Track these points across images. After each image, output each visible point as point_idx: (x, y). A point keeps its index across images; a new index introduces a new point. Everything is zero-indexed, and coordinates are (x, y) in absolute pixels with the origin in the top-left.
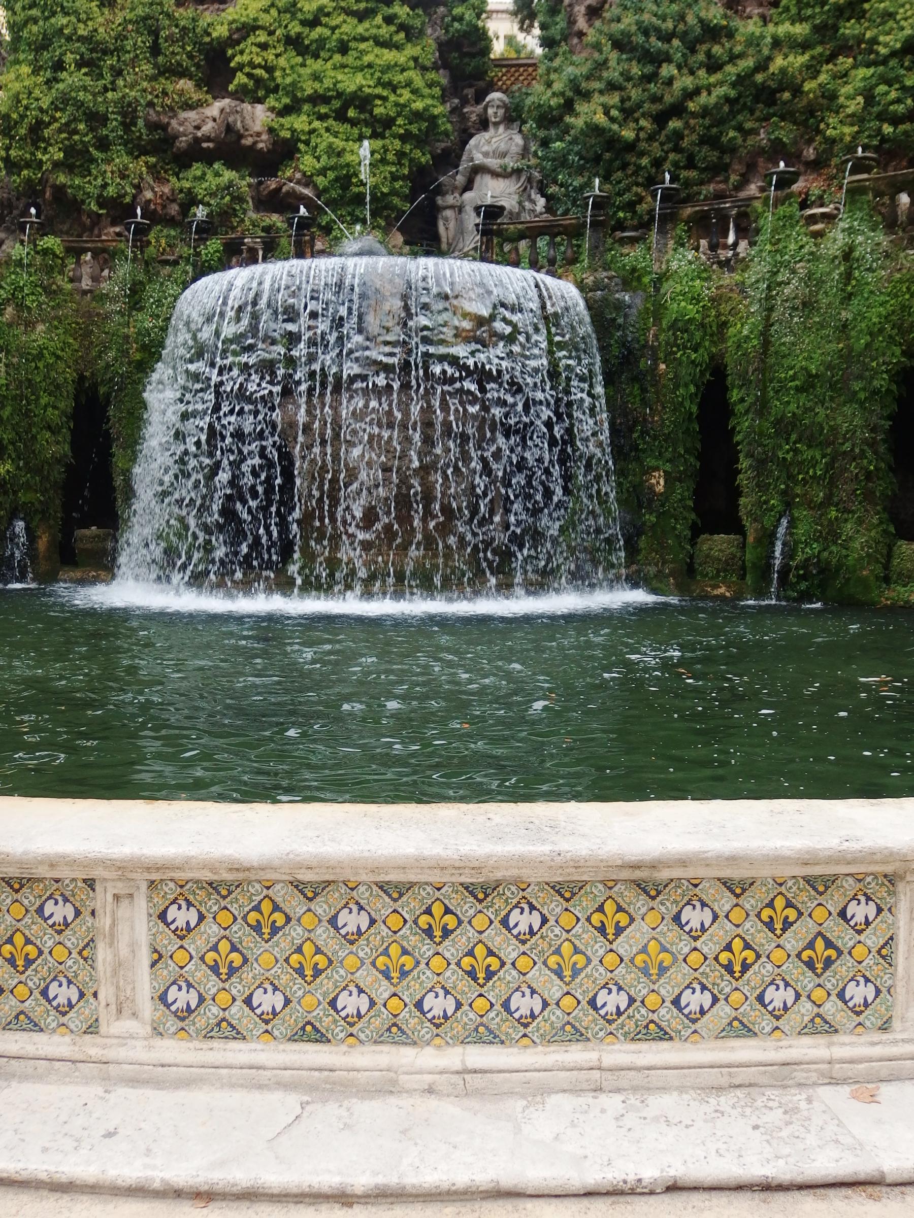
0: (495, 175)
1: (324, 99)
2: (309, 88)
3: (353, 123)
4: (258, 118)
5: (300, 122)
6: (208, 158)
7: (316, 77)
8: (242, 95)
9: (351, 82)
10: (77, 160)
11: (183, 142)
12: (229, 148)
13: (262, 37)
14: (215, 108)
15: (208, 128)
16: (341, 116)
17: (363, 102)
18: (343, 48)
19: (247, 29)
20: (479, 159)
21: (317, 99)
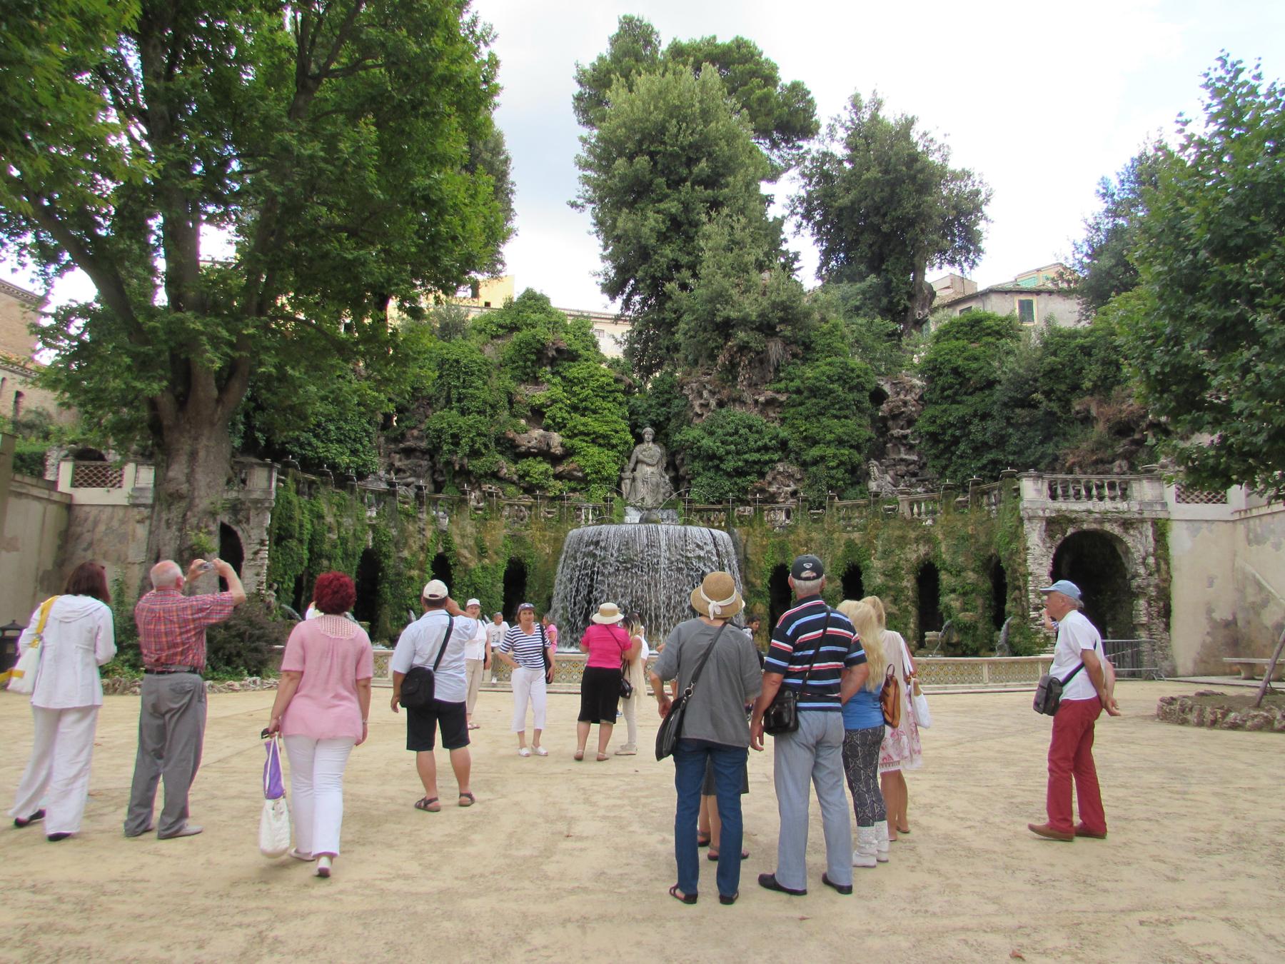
0: (648, 465)
1: (588, 434)
2: (582, 428)
3: (600, 445)
4: (556, 438)
5: (576, 442)
6: (535, 455)
7: (583, 424)
8: (547, 428)
9: (603, 429)
10: (475, 454)
11: (523, 449)
12: (545, 454)
13: (560, 405)
14: (537, 433)
15: (534, 443)
16: (593, 441)
17: (605, 437)
18: (595, 412)
19: (554, 401)
20: (641, 457)
21: (582, 433)
